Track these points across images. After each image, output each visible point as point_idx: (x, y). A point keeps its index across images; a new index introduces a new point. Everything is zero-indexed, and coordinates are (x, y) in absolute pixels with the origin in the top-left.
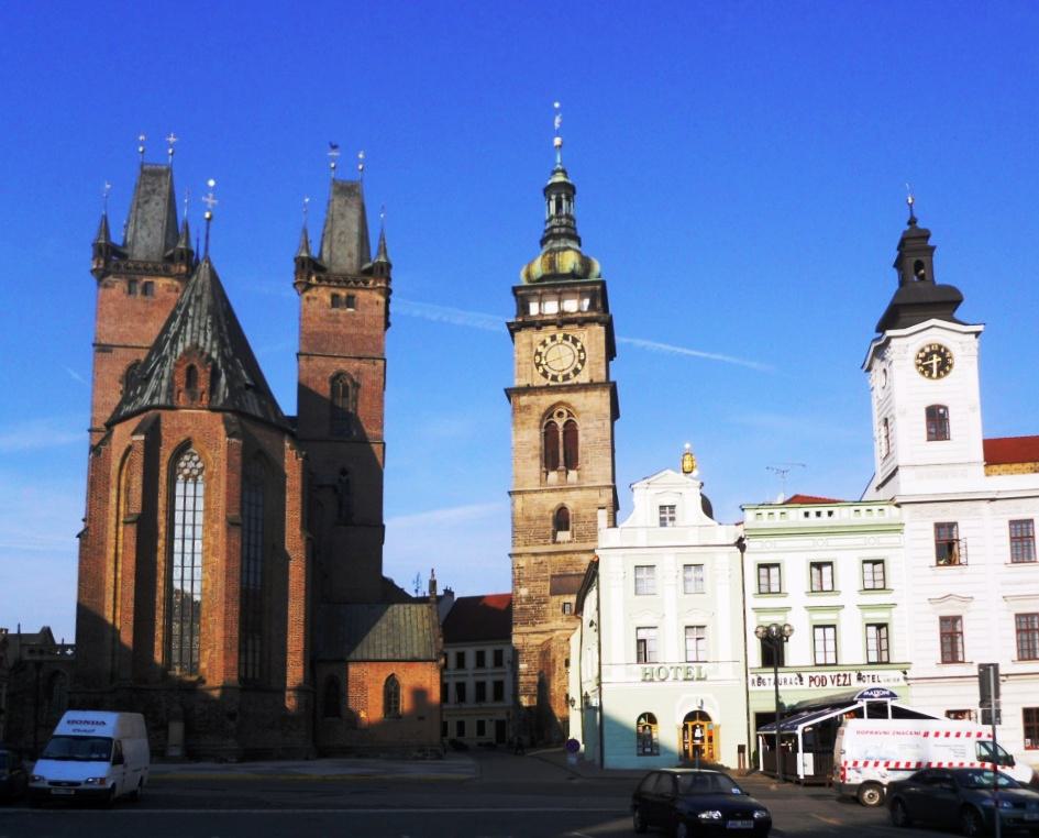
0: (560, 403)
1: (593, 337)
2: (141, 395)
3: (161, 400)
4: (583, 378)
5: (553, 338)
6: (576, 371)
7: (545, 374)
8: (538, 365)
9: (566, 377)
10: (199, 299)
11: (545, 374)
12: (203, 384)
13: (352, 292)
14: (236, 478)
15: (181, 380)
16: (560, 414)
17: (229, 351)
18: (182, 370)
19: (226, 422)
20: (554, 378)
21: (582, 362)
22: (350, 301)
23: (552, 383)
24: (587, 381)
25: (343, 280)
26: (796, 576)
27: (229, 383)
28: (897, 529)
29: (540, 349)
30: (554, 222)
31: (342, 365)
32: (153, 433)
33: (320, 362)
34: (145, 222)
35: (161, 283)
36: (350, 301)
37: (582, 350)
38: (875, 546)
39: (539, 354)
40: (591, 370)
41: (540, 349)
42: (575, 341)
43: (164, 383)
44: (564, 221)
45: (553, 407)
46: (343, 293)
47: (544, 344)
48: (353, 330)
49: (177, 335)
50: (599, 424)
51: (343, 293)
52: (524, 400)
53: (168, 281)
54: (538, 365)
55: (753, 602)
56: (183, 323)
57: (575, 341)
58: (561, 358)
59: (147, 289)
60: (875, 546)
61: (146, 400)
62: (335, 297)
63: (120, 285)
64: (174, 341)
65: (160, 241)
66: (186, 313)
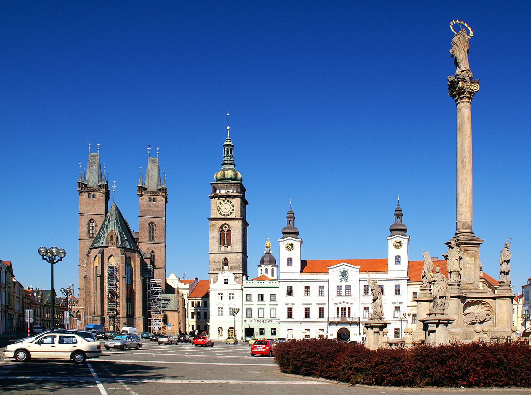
0: (226, 224)
1: (237, 202)
2: (99, 242)
3: (104, 245)
4: (233, 216)
5: (224, 201)
6: (231, 213)
7: (221, 213)
8: (219, 210)
9: (228, 215)
10: (112, 215)
11: (221, 213)
12: (115, 241)
13: (155, 197)
14: (124, 265)
15: (109, 239)
16: (226, 227)
17: (121, 230)
18: (109, 237)
19: (121, 251)
20: (224, 215)
21: (233, 210)
22: (154, 200)
23: (223, 217)
24: (234, 217)
25: (152, 193)
26: (255, 297)
27: (121, 239)
28: (278, 287)
29: (219, 205)
30: (226, 158)
31: (152, 220)
32: (103, 253)
33: (146, 219)
34: (92, 173)
35: (98, 194)
36: (154, 200)
37: (233, 206)
38: (273, 291)
39: (218, 206)
40: (236, 213)
41: (219, 205)
42: (231, 203)
43: (105, 240)
44: (229, 158)
45: (223, 225)
46: (152, 197)
47: (220, 203)
48: (155, 209)
49: (107, 225)
50: (238, 231)
51: (152, 197)
52: (213, 222)
53: (100, 193)
54: (219, 210)
55: (245, 303)
56: (109, 222)
57: (231, 203)
58: (226, 207)
59: (94, 196)
60: (273, 291)
61: (100, 244)
62: (150, 198)
63: (86, 195)
64: (107, 228)
65: (97, 180)
66: (109, 219)
